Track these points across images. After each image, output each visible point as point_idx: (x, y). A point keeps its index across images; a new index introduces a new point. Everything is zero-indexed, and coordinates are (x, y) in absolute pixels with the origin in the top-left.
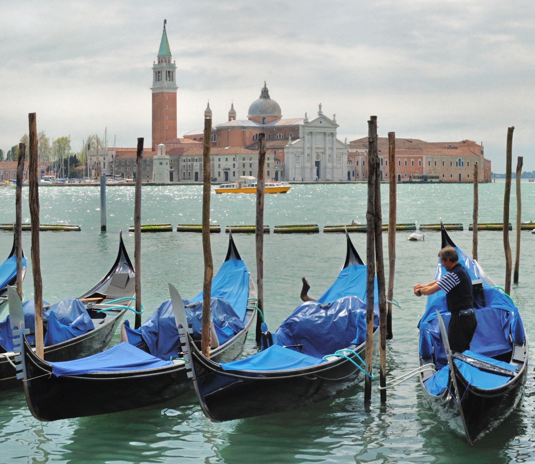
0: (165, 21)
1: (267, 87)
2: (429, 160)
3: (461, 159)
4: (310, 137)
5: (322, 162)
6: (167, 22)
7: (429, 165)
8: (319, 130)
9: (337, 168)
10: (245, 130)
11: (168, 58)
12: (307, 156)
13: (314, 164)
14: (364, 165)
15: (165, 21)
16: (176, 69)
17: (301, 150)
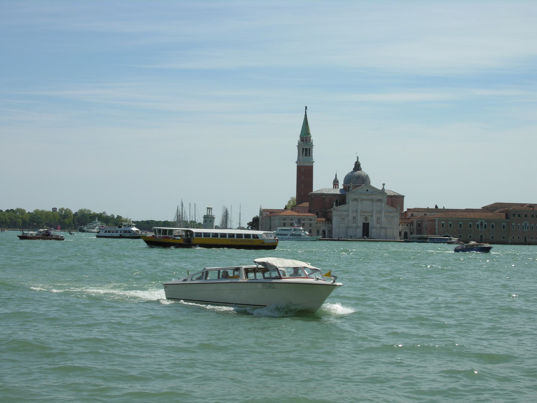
0: (306, 107)
1: (359, 160)
2: (443, 222)
3: (484, 222)
4: (355, 203)
5: (370, 223)
6: (307, 108)
7: (443, 226)
8: (364, 197)
9: (385, 228)
10: (324, 196)
11: (306, 137)
12: (351, 218)
13: (360, 225)
14: (419, 226)
15: (306, 107)
16: (313, 146)
17: (345, 213)
